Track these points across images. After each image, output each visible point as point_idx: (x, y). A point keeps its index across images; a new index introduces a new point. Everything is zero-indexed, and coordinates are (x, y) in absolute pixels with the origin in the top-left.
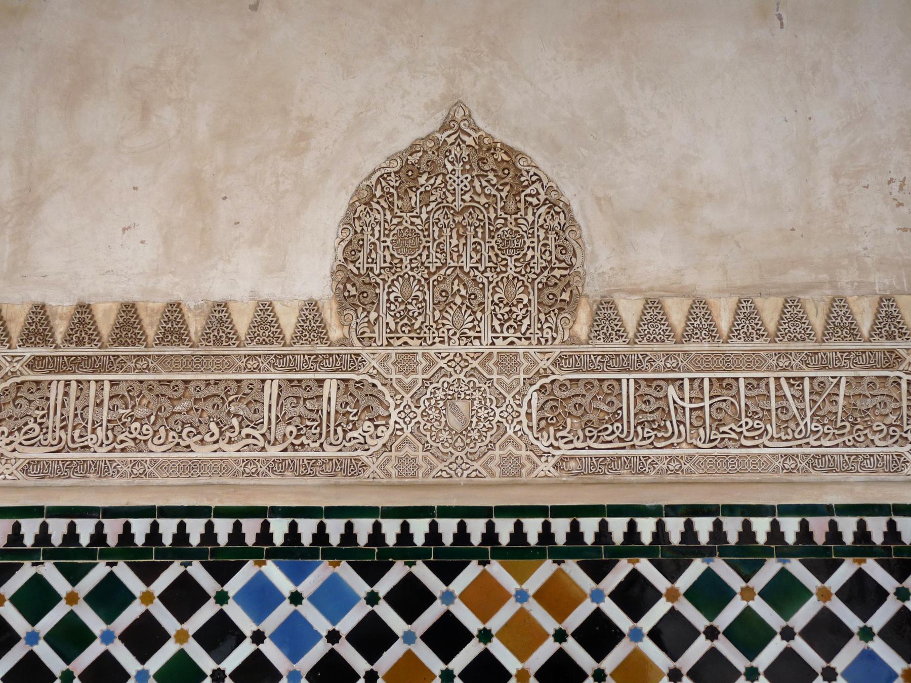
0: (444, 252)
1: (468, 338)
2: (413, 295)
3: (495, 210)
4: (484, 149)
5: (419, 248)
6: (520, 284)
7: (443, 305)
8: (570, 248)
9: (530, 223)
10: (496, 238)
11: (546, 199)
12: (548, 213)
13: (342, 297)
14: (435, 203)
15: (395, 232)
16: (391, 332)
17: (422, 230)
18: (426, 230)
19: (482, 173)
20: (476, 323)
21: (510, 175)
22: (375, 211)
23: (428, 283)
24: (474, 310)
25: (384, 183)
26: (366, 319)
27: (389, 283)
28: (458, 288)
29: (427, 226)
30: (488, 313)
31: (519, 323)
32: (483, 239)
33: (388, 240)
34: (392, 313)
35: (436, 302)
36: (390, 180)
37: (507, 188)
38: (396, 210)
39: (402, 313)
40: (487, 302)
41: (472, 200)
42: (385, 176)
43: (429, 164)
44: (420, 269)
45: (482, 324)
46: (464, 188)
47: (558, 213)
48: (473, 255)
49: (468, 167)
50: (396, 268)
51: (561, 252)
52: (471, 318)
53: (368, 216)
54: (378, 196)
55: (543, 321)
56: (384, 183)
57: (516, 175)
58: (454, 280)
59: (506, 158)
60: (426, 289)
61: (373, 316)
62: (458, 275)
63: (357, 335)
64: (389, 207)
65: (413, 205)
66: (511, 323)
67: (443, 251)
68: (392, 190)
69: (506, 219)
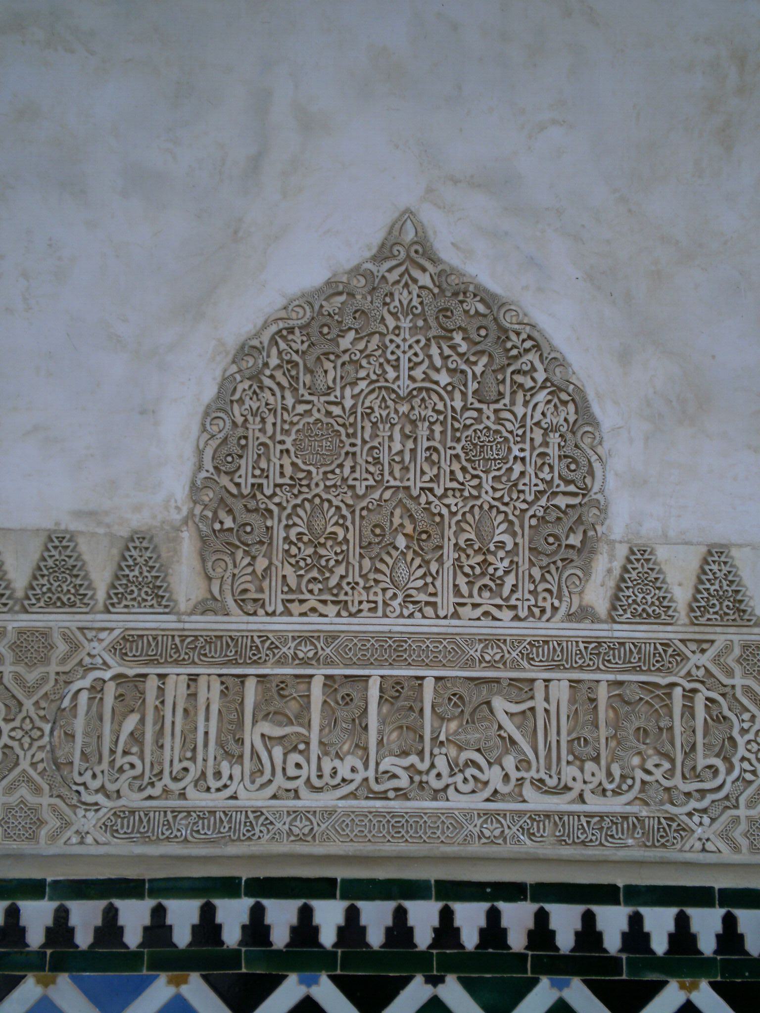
0: (379, 463)
3: (464, 394)
4: (449, 294)
5: (340, 455)
6: (501, 517)
7: (377, 549)
8: (583, 461)
9: (519, 417)
10: (463, 442)
11: (546, 380)
12: (549, 402)
15: (300, 426)
16: (291, 590)
18: (351, 424)
19: (443, 333)
20: (429, 580)
21: (489, 339)
22: (267, 390)
23: (353, 513)
24: (427, 557)
25: (283, 345)
26: (250, 569)
27: (289, 510)
28: (400, 521)
30: (448, 564)
31: (498, 582)
32: (443, 442)
33: (289, 440)
34: (293, 561)
35: (364, 544)
37: (484, 360)
38: (302, 391)
39: (309, 561)
41: (427, 378)
42: (285, 333)
43: (357, 315)
45: (438, 583)
46: (414, 359)
47: (565, 403)
48: (426, 468)
50: (301, 486)
51: (568, 467)
52: (420, 572)
53: (255, 397)
54: (272, 366)
57: (499, 338)
58: (394, 508)
59: (481, 308)
61: (261, 564)
62: (401, 501)
63: (233, 595)
65: (331, 385)
66: (486, 581)
67: (377, 461)
68: (295, 357)
69: (479, 411)
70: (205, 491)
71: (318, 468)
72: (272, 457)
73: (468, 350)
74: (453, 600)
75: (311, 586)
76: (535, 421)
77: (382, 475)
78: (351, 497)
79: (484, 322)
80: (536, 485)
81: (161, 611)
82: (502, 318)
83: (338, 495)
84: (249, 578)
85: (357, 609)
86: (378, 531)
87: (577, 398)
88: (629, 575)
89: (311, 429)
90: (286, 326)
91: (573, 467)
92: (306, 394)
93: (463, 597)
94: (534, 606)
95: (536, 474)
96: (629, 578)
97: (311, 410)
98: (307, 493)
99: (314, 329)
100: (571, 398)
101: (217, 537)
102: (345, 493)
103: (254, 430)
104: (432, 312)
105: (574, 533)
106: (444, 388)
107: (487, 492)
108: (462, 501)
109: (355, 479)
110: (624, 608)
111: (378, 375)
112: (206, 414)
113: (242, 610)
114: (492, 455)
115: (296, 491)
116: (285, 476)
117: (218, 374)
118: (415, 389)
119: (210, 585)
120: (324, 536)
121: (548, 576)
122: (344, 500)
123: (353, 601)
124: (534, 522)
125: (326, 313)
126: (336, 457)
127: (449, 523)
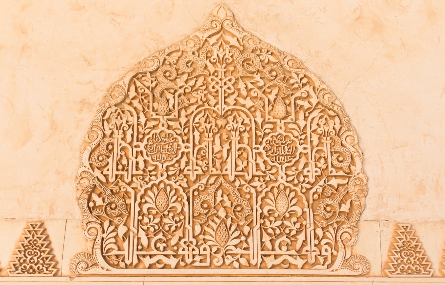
1: (233, 255)
5: (176, 154)
6: (292, 195)
10: (264, 145)
11: (318, 103)
12: (321, 117)
13: (86, 208)
14: (195, 107)
15: (150, 136)
17: (180, 135)
20: (243, 238)
21: (278, 78)
26: (114, 234)
27: (142, 192)
28: (222, 199)
29: (186, 131)
31: (292, 239)
36: (145, 80)
40: (256, 216)
43: (189, 65)
44: (178, 178)
45: (250, 240)
46: (227, 90)
52: (237, 234)
53: (119, 118)
54: (131, 96)
56: (138, 84)
57: (284, 77)
58: (217, 190)
59: (272, 59)
60: (185, 200)
61: (122, 230)
62: (221, 184)
63: (102, 253)
64: (143, 108)
68: (147, 91)
71: (162, 164)
72: (130, 156)
73: (264, 85)
75: (158, 245)
76: (312, 130)
77: (208, 167)
79: (275, 67)
80: (316, 172)
83: (177, 181)
86: (205, 206)
87: (340, 113)
89: (158, 137)
91: (341, 159)
92: (154, 114)
94: (319, 255)
97: (158, 124)
99: (159, 74)
100: (335, 114)
101: (91, 213)
102: (182, 180)
107: (282, 178)
108: (265, 184)
114: (285, 153)
115: (147, 179)
116: (139, 169)
118: (229, 110)
120: (167, 210)
121: (328, 234)
122: (182, 185)
124: (316, 196)
125: (168, 63)
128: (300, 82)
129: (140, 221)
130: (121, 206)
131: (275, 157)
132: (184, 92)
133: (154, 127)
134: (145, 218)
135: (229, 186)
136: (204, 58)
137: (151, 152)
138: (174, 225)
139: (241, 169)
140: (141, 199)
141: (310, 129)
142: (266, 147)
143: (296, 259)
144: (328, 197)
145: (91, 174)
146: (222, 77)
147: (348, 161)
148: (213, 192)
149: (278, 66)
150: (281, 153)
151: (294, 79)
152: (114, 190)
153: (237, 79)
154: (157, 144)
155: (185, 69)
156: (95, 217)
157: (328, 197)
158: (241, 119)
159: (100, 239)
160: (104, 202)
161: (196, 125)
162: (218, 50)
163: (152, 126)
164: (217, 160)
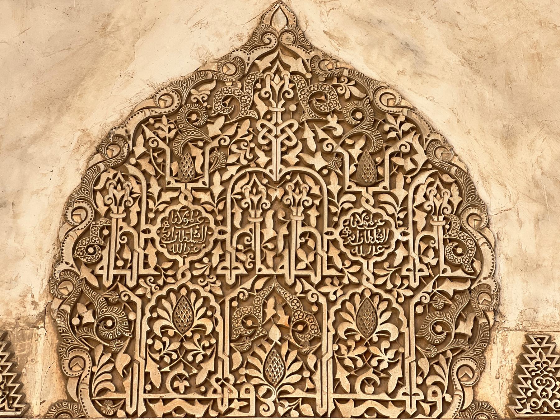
0: (250, 250)
1: (290, 400)
2: (196, 323)
3: (341, 179)
5: (206, 243)
8: (470, 244)
9: (400, 201)
10: (341, 227)
11: (427, 162)
12: (431, 184)
14: (236, 168)
15: (166, 214)
16: (154, 389)
18: (220, 212)
19: (317, 117)
20: (306, 374)
21: (365, 122)
22: (132, 179)
23: (222, 304)
25: (149, 133)
26: (110, 367)
27: (153, 303)
28: (274, 312)
29: (221, 206)
30: (327, 356)
31: (383, 375)
33: (154, 229)
34: (157, 357)
35: (234, 337)
36: (159, 128)
38: (168, 178)
39: (174, 356)
43: (227, 102)
45: (317, 377)
46: (287, 143)
47: (448, 185)
48: (302, 254)
49: (293, 108)
50: (166, 276)
51: (454, 251)
52: (296, 366)
53: (119, 187)
55: (426, 371)
56: (149, 133)
57: (376, 121)
58: (267, 298)
59: (356, 92)
60: (218, 315)
61: (122, 360)
63: (91, 396)
64: (156, 171)
65: (199, 171)
66: (370, 374)
67: (248, 249)
68: (162, 145)
70: (63, 285)
71: (184, 258)
72: (136, 247)
73: (344, 133)
74: (333, 396)
75: (176, 384)
76: (415, 205)
77: (254, 263)
78: (221, 287)
79: (360, 106)
80: (421, 270)
81: (13, 413)
82: (378, 102)
83: (207, 285)
84: (109, 377)
85: (227, 407)
86: (249, 323)
88: (527, 366)
89: (177, 216)
90: (154, 114)
91: (459, 251)
92: (173, 181)
93: (346, 393)
94: (423, 401)
95: (420, 259)
96: (527, 369)
97: (178, 197)
98: (174, 283)
99: (181, 116)
101: (75, 333)
102: (214, 283)
103: (117, 219)
104: (305, 96)
105: (465, 320)
106: (320, 172)
107: (368, 279)
108: (341, 289)
109: (224, 268)
110: (523, 402)
111: (249, 161)
112: (68, 204)
113: (100, 412)
114: (373, 240)
115: (160, 282)
116: (150, 267)
117: (82, 165)
118: (288, 173)
119: (66, 386)
120: (191, 329)
121: (437, 368)
122: (213, 290)
123: (222, 400)
124: (420, 310)
125: (195, 100)
126: (204, 245)
127: (328, 313)
128: (398, 129)
129: (150, 347)
130: (120, 323)
131: (357, 248)
132: (218, 145)
133: (174, 200)
134: (157, 341)
135: (285, 293)
136: (250, 92)
137: (166, 241)
138: (200, 353)
139: (304, 267)
140: (151, 314)
141: (413, 202)
142: (345, 232)
143: (387, 407)
144: (440, 310)
145: (76, 273)
146: (278, 121)
147: (471, 255)
148: (260, 301)
149: (365, 103)
150: (367, 240)
151: (389, 123)
152: (110, 299)
153: (302, 124)
154: (176, 227)
155: (221, 108)
156: (80, 340)
157: (440, 310)
158: (306, 188)
159: (88, 374)
160: (94, 316)
161: (236, 196)
162: (272, 78)
163: (169, 200)
164: (268, 252)
